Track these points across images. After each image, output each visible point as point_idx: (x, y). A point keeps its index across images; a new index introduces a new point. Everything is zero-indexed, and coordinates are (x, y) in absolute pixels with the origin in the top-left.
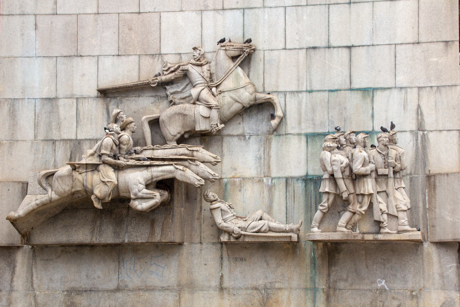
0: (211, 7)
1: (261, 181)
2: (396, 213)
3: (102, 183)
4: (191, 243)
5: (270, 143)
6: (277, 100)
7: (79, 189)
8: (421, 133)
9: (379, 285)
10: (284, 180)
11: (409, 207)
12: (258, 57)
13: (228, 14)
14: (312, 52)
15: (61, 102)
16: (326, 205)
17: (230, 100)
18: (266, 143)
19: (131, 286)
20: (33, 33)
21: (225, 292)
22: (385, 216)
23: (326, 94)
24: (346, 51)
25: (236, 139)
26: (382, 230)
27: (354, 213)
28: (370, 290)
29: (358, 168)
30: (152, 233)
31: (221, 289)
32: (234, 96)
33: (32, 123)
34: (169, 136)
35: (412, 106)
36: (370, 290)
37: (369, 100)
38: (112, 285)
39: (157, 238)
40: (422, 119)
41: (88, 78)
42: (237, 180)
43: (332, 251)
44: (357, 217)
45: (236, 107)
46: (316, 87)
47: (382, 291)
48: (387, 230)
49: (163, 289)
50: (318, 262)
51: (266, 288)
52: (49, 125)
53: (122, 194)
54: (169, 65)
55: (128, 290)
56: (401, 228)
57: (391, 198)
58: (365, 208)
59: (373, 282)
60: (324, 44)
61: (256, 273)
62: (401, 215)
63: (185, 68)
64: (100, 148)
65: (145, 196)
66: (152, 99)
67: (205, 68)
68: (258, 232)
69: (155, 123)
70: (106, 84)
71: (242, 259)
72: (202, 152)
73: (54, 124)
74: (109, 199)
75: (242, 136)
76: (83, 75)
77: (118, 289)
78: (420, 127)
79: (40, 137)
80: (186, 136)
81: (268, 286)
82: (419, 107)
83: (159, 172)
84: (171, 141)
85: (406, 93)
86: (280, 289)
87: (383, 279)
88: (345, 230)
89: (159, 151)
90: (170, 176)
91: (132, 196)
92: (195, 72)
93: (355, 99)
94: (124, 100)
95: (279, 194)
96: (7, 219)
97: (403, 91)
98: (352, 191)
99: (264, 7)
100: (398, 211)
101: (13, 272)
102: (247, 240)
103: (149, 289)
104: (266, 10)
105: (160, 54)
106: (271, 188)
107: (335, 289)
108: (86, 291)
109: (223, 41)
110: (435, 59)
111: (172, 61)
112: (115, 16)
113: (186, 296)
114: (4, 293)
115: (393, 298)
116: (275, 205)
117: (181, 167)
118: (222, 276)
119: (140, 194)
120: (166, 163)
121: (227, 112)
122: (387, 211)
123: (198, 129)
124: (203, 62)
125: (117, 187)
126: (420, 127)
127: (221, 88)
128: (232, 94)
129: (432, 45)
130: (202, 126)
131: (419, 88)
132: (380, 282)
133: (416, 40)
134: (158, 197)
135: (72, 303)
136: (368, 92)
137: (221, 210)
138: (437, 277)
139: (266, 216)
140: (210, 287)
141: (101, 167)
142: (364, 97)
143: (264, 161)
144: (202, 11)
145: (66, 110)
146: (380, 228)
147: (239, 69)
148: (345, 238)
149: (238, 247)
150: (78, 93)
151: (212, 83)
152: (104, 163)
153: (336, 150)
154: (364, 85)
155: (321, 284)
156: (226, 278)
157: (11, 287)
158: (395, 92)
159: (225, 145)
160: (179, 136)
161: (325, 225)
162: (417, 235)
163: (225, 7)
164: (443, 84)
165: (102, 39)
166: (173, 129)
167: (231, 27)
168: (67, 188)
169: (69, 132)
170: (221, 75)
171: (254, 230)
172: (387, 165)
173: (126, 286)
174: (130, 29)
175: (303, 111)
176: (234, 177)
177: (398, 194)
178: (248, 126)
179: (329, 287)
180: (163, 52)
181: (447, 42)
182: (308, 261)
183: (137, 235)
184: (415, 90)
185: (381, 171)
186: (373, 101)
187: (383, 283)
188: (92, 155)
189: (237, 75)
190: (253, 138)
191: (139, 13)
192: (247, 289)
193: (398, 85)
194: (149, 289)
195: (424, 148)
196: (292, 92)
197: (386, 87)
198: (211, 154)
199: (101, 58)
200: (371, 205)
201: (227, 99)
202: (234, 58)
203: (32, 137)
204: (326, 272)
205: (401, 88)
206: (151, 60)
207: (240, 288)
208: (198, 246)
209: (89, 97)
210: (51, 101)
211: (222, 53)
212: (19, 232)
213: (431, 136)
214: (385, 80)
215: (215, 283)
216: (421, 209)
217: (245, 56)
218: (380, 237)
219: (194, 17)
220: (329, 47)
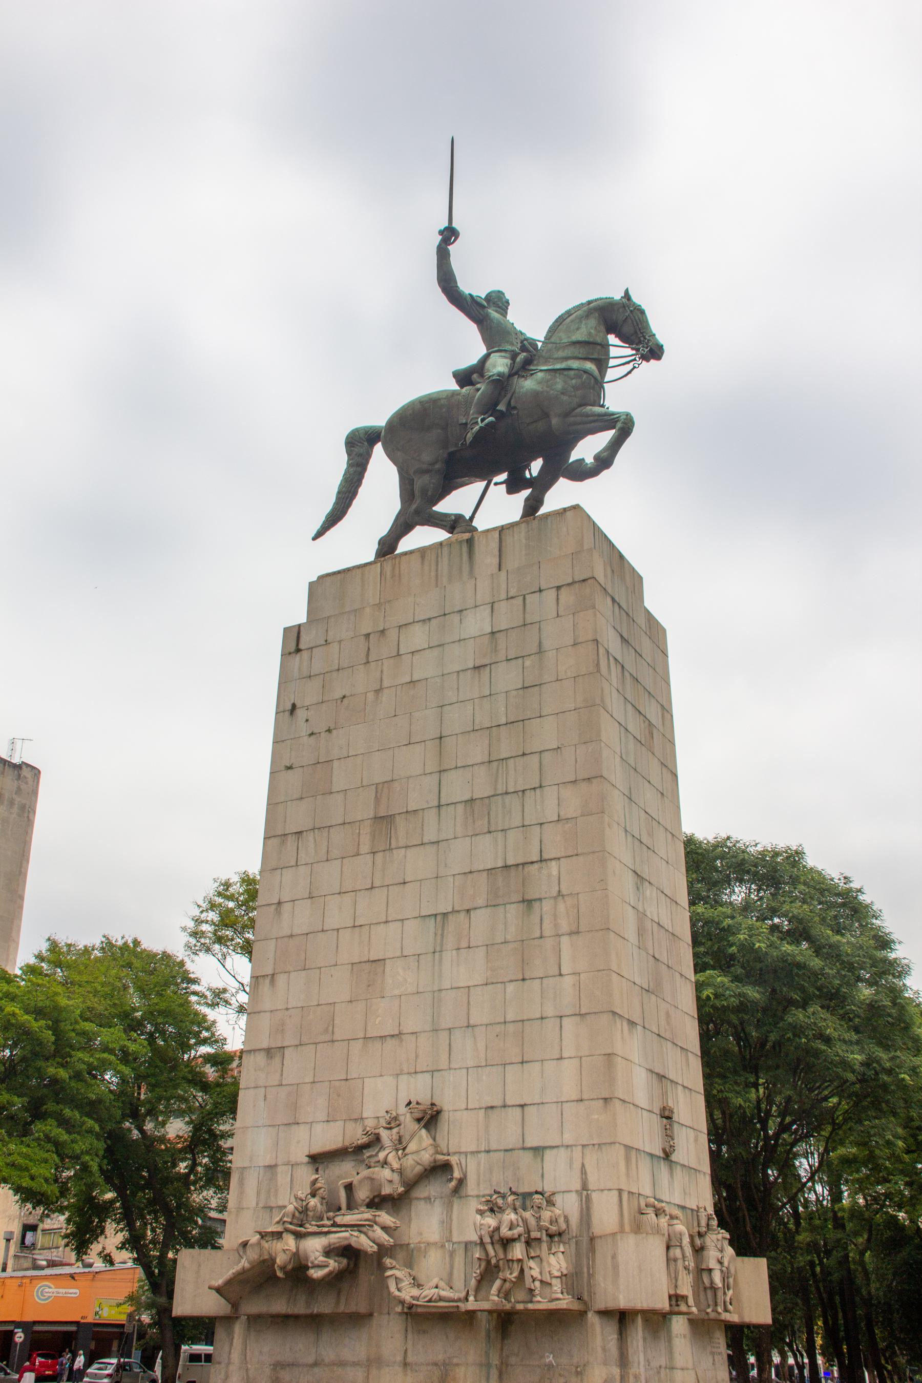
0: (406, 1071)
1: (443, 1246)
2: (549, 1280)
4: (381, 1313)
5: (452, 1206)
6: (454, 1160)
7: (266, 1257)
8: (585, 1192)
9: (547, 1360)
10: (463, 1246)
11: (565, 1272)
12: (444, 1116)
13: (420, 1076)
14: (490, 1111)
15: (280, 1169)
16: (478, 1271)
17: (412, 1162)
18: (449, 1206)
19: (327, 1361)
20: (262, 1103)
21: (408, 1368)
22: (537, 1283)
23: (502, 1153)
24: (519, 1110)
25: (422, 1202)
26: (535, 1299)
27: (505, 1280)
28: (539, 1366)
29: (505, 1232)
30: (338, 1303)
31: (405, 1364)
32: (416, 1158)
33: (255, 1191)
34: (359, 1201)
35: (577, 1165)
36: (539, 1366)
37: (539, 1160)
38: (310, 1360)
39: (342, 1309)
40: (586, 1178)
42: (422, 1245)
43: (506, 1322)
44: (507, 1285)
45: (419, 1169)
46: (494, 1146)
47: (550, 1366)
48: (539, 1298)
49: (355, 1364)
50: (493, 1335)
51: (444, 1364)
52: (269, 1192)
53: (303, 1262)
54: (368, 1129)
55: (325, 1365)
56: (554, 1296)
57: (545, 1263)
58: (515, 1274)
59: (542, 1357)
60: (500, 1103)
61: (435, 1348)
62: (554, 1281)
63: (377, 1131)
64: (284, 1216)
65: (320, 1264)
66: (353, 1164)
67: (395, 1130)
68: (430, 1301)
69: (349, 1187)
70: (317, 1149)
71: (424, 1332)
72: (385, 1218)
73: (273, 1190)
74: (290, 1267)
75: (428, 1199)
76: (298, 1142)
77: (315, 1364)
78: (585, 1187)
79: (261, 1205)
80: (376, 1200)
81: (447, 1361)
82: (583, 1165)
83: (338, 1238)
84: (361, 1206)
85: (572, 1151)
86: (457, 1365)
87: (551, 1353)
88: (496, 1298)
89: (349, 1217)
90: (345, 1243)
91: (310, 1264)
92: (384, 1134)
93: (526, 1158)
94: (330, 1165)
95: (459, 1260)
96: (210, 1288)
97: (569, 1149)
98: (501, 1256)
99: (450, 1069)
100: (551, 1278)
101: (231, 1344)
102: (419, 1310)
103: (342, 1364)
104: (452, 1071)
105: (362, 1118)
106: (452, 1254)
107: (507, 1365)
108: (288, 1365)
109: (409, 1103)
110: (596, 1117)
111: (370, 1124)
112: (327, 1084)
113: (374, 1371)
114: (223, 1365)
115: (560, 1375)
116: (455, 1272)
117: (356, 1234)
118: (406, 1350)
119: (316, 1262)
120: (343, 1229)
121: (411, 1174)
122: (539, 1277)
123: (383, 1193)
124: (392, 1125)
125: (296, 1255)
126: (585, 1187)
127: (407, 1151)
128: (415, 1157)
129: (593, 1102)
130: (386, 1190)
131: (584, 1146)
132: (548, 1357)
133: (579, 1097)
134: (333, 1264)
135: (277, 1378)
136: (538, 1151)
137: (396, 1278)
138: (599, 1350)
139: (442, 1284)
140: (395, 1362)
141: (284, 1235)
142: (535, 1156)
143: (447, 1225)
144: (397, 1075)
145: (283, 1177)
146: (534, 1296)
147: (424, 1131)
148: (495, 1308)
149: (426, 1319)
150: (293, 1159)
151: (400, 1144)
152: (287, 1230)
153: (488, 1213)
154: (535, 1144)
155: (495, 1361)
156: (409, 1353)
157: (229, 1359)
158: (562, 1150)
159: (413, 1207)
160: (368, 1200)
161: (482, 1294)
163: (418, 1070)
164: (604, 1141)
165: (315, 1106)
166: (362, 1194)
167: (418, 1089)
168: (256, 1257)
170: (407, 1137)
171: (426, 1299)
172: (540, 1228)
173: (323, 1360)
174: (339, 1096)
175: (482, 1172)
176: (419, 1243)
177: (552, 1260)
178: (434, 1188)
179: (502, 1363)
180: (365, 1115)
181: (605, 1099)
182: (483, 1334)
183: (324, 1306)
184: (580, 1148)
185: (534, 1234)
186: (542, 1160)
187: (550, 1358)
188: (278, 1222)
189: (421, 1137)
190: (437, 1201)
191: (347, 1080)
192: (428, 1365)
193: (566, 1142)
194: (342, 1364)
195: (588, 1208)
196: (472, 1153)
197: (554, 1145)
198: (392, 1219)
199: (314, 1124)
200: (522, 1271)
201: (409, 1161)
202: (419, 1120)
203: (254, 1204)
204: (499, 1346)
205: (567, 1146)
206: (354, 1125)
207: (422, 1364)
208: (387, 1316)
209: (302, 1163)
210: (272, 1168)
211: (408, 1115)
212: (228, 1301)
213: (595, 1196)
214: (552, 1139)
215: (399, 1358)
216: (586, 1275)
217: (430, 1118)
218: (530, 1306)
219: (390, 1080)
220: (505, 1106)
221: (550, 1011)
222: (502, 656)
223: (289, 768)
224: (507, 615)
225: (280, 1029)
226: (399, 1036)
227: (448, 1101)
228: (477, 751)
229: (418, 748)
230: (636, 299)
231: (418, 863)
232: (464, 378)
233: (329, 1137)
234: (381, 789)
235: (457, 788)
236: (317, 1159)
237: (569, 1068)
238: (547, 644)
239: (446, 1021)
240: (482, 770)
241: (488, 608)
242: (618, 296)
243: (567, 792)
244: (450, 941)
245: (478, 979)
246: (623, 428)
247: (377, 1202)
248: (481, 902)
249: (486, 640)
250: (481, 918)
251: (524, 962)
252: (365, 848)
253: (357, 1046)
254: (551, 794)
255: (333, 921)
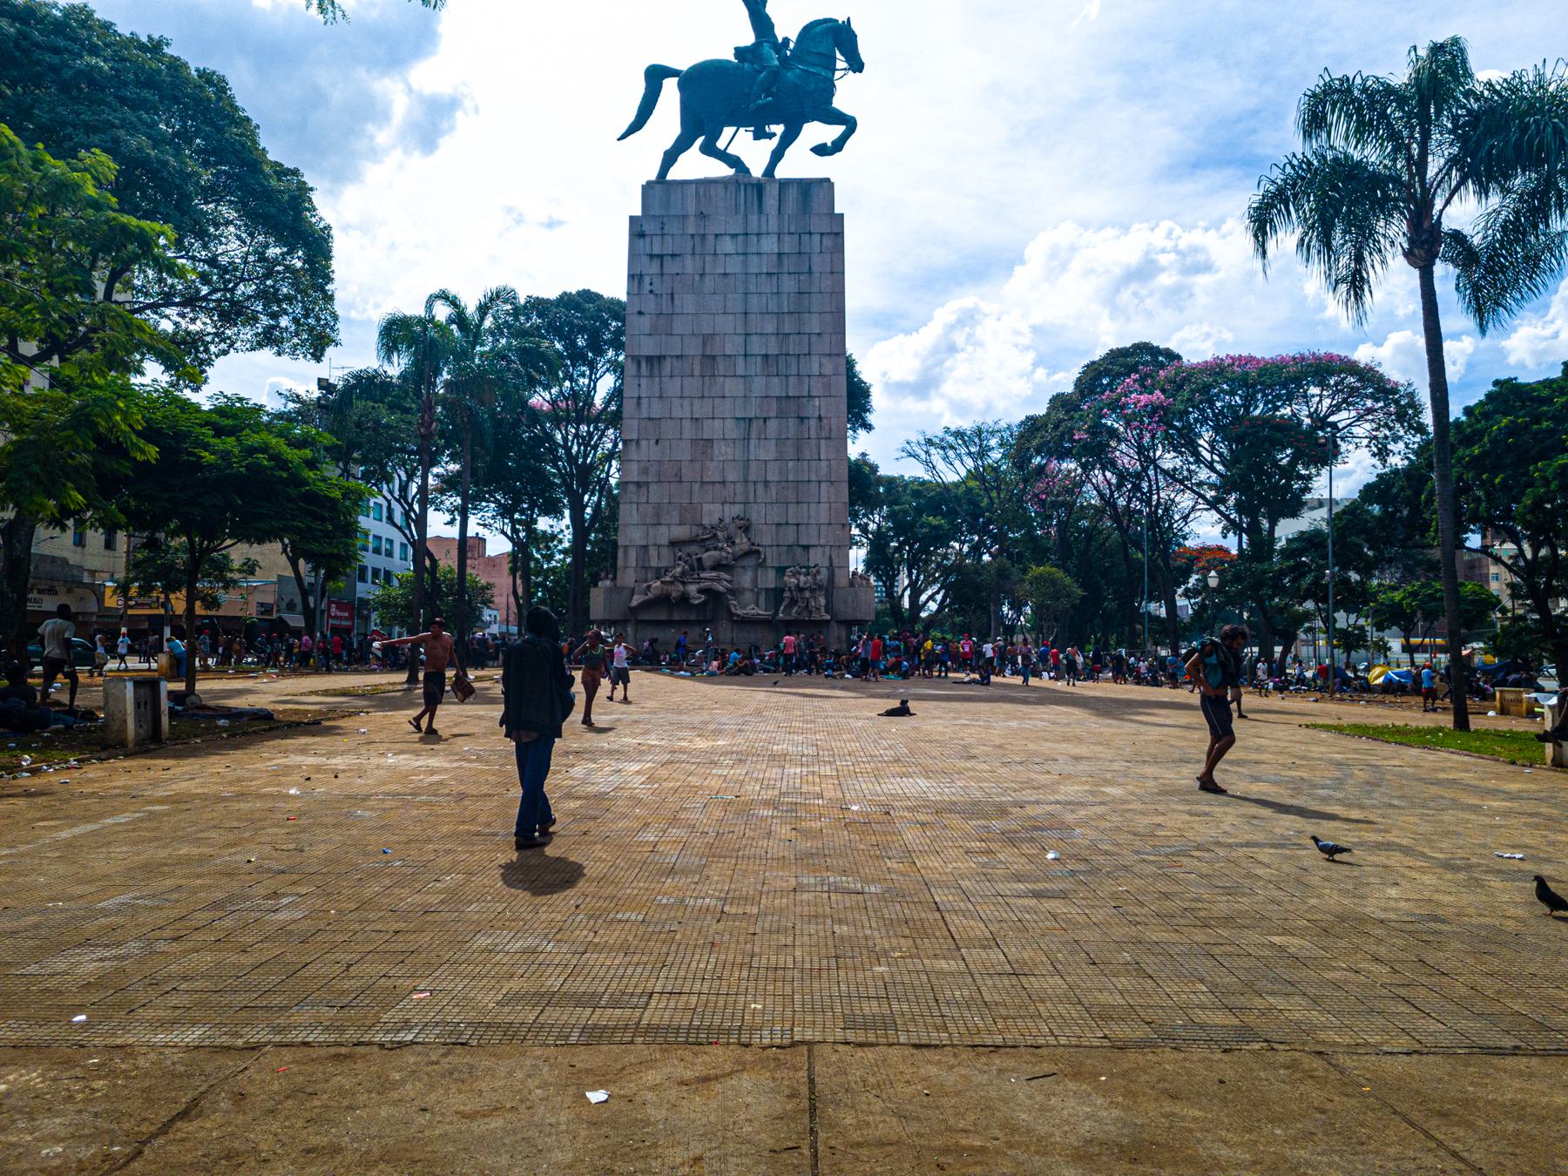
3: (676, 591)
41: (664, 535)
93: (799, 550)
136: (806, 548)
143: (755, 581)
145: (653, 552)
162: (828, 617)
167: (737, 510)
169: (654, 563)
210: (646, 547)
214: (814, 541)
217: (746, 529)
221: (813, 478)
222: (785, 269)
223: (640, 313)
224: (789, 245)
225: (645, 471)
226: (724, 482)
227: (754, 517)
228: (770, 327)
229: (731, 317)
230: (853, 26)
231: (733, 387)
232: (739, 52)
233: (682, 532)
234: (707, 339)
235: (757, 346)
236: (673, 544)
237: (824, 507)
238: (814, 268)
239: (752, 477)
240: (773, 338)
241: (775, 239)
242: (841, 19)
243: (825, 360)
244: (754, 434)
245: (771, 456)
246: (850, 124)
247: (718, 566)
248: (773, 414)
249: (775, 258)
250: (773, 425)
251: (799, 450)
252: (697, 373)
253: (696, 487)
254: (815, 359)
255: (677, 413)
